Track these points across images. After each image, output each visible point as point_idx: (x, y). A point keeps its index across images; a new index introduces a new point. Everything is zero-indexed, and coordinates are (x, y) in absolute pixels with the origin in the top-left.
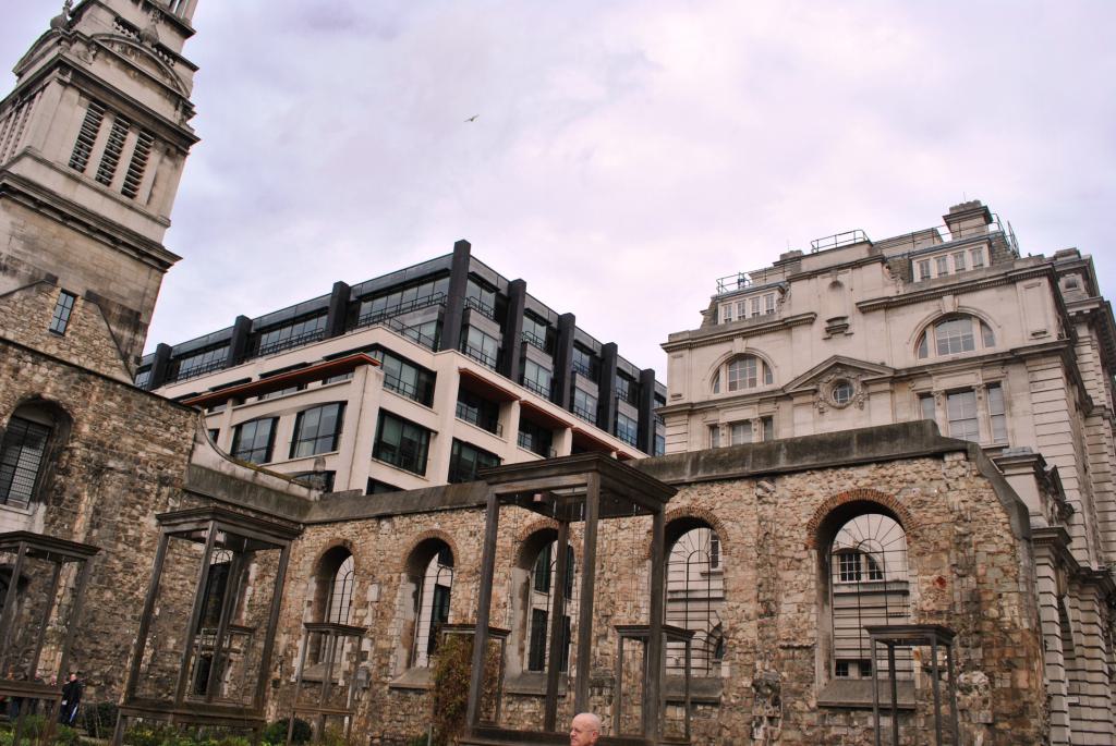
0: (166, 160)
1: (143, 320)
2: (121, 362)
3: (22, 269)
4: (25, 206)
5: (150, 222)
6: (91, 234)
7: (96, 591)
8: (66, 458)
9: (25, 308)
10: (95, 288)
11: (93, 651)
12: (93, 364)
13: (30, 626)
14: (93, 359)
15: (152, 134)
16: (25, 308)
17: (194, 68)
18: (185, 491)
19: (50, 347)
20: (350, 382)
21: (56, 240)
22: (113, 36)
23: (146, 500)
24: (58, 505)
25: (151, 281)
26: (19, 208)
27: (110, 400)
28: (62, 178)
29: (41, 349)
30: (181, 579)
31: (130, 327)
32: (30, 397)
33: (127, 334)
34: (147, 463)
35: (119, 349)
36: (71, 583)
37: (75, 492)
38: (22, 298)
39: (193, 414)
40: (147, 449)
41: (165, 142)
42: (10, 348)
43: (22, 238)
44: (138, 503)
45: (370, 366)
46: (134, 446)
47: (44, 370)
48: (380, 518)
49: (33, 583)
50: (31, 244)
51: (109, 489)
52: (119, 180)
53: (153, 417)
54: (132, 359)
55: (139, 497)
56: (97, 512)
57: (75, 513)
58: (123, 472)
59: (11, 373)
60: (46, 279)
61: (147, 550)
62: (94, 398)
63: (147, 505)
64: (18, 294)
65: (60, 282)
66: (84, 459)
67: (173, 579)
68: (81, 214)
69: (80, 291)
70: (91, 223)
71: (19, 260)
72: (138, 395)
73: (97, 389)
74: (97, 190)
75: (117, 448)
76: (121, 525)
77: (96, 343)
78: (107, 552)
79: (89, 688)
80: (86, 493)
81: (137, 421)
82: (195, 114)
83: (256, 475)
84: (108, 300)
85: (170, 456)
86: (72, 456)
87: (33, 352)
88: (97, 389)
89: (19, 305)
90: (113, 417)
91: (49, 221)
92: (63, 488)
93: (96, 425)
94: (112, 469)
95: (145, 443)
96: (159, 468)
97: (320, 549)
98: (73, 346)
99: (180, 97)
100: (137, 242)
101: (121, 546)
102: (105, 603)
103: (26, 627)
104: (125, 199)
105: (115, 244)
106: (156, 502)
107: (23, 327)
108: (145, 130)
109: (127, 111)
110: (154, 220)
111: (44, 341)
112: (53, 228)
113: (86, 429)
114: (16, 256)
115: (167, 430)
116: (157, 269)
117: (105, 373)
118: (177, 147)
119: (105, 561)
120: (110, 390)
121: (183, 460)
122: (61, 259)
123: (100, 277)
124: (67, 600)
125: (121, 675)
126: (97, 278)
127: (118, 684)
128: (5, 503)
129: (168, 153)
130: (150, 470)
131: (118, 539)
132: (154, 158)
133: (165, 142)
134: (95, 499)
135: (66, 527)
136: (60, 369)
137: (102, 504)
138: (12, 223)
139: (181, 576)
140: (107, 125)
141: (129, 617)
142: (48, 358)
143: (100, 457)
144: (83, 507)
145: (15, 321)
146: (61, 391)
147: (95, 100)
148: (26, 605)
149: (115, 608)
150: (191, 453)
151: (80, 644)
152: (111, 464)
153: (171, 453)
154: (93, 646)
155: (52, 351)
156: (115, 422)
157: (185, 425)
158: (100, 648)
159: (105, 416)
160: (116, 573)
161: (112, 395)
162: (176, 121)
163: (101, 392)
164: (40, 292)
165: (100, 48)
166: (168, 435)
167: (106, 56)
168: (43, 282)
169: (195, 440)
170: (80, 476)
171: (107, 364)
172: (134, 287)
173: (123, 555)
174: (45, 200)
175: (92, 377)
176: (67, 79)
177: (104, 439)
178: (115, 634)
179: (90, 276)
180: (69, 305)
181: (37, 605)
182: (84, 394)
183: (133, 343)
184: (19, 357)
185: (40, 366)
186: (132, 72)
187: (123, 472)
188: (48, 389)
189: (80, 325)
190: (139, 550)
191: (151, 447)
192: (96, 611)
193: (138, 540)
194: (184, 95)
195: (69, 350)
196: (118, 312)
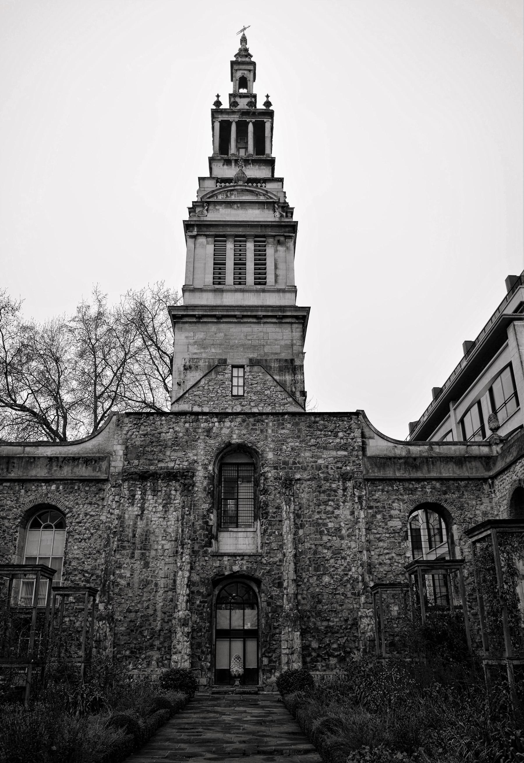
0: (280, 248)
1: (297, 363)
2: (290, 399)
3: (201, 363)
4: (190, 322)
5: (281, 294)
6: (239, 320)
7: (315, 578)
8: (262, 481)
9: (210, 387)
10: (254, 355)
11: (326, 627)
12: (270, 408)
13: (270, 615)
14: (269, 404)
15: (264, 236)
16: (210, 387)
17: (281, 180)
18: (368, 480)
19: (235, 408)
20: (507, 345)
21: (218, 335)
22: (213, 191)
23: (336, 496)
24: (266, 518)
25: (294, 333)
26: (187, 326)
27: (283, 428)
28: (210, 295)
29: (229, 411)
30: (388, 553)
31: (288, 372)
32: (223, 446)
33: (288, 378)
34: (327, 467)
35: (285, 390)
36: (292, 576)
37: (276, 505)
38: (206, 382)
39: (354, 417)
40: (325, 456)
41: (274, 236)
42: (200, 417)
43: (195, 343)
44: (329, 500)
45: (516, 323)
46: (312, 457)
47: (228, 424)
49: (264, 582)
50: (202, 345)
51: (303, 495)
52: (250, 278)
53: (321, 431)
54: (298, 394)
55: (329, 495)
56: (298, 516)
57: (281, 521)
58: (309, 480)
59: (205, 434)
60: (219, 363)
61: (348, 536)
62: (270, 431)
63: (338, 500)
64: (203, 380)
65: (229, 361)
66: (275, 479)
67: (379, 555)
68: (227, 311)
69: (244, 361)
70: (237, 313)
71: (197, 358)
72: (303, 418)
73: (271, 424)
74: (236, 291)
75: (299, 462)
76: (320, 521)
77: (266, 392)
78: (316, 545)
79: (331, 658)
80: (284, 503)
81: (309, 438)
82: (293, 208)
83: (432, 449)
84: (266, 360)
85: (345, 456)
86: (266, 479)
87: (217, 414)
88: (271, 424)
89: (206, 388)
90: (289, 440)
91: (210, 325)
92: (267, 505)
93: (278, 450)
94: (299, 479)
95: (320, 452)
96: (338, 468)
97: (507, 495)
98: (252, 401)
99: (274, 203)
100: (272, 311)
101: (325, 538)
102: (326, 586)
103: (267, 614)
104: (259, 287)
105: (259, 319)
106: (344, 495)
107: (214, 401)
108: (257, 236)
109: (240, 231)
110: (283, 291)
111: (229, 405)
112: (213, 328)
113: (270, 456)
114: (195, 356)
115: (336, 436)
116: (295, 323)
117: (281, 411)
118: (284, 236)
119: (315, 553)
120: (281, 421)
121: (357, 456)
123: (255, 346)
124: (291, 590)
125: (357, 644)
126: (254, 347)
127: (356, 652)
128: (237, 527)
129: (279, 242)
130: (331, 472)
131: (321, 533)
132: (270, 251)
133: (274, 236)
134: (292, 507)
135: (277, 533)
136: (239, 420)
137: (300, 509)
138: (187, 337)
139: (386, 551)
140: (230, 246)
141: (349, 595)
142: (227, 414)
143: (287, 473)
144: (284, 514)
145: (206, 399)
146: (244, 435)
147: (216, 236)
148: (262, 599)
149: (336, 589)
150: (363, 448)
151: (315, 624)
152: (298, 476)
153: (345, 453)
154: (325, 623)
155: (238, 409)
156: (293, 443)
157: (350, 428)
158: (331, 624)
159: (284, 441)
160: (327, 560)
161: (283, 424)
162: (277, 219)
163: (274, 425)
164: (217, 373)
165: (209, 203)
166: (338, 440)
167: (215, 206)
168: (217, 366)
169: (363, 436)
170: (277, 491)
171: (280, 405)
172: (283, 343)
173: (329, 545)
174: (201, 313)
175: (264, 417)
176: (195, 233)
177: (287, 459)
178: (342, 611)
179: (247, 348)
180: (241, 374)
181: (271, 598)
182: (262, 431)
183: (295, 382)
184: (206, 421)
185: (224, 422)
186: (236, 206)
187: (309, 480)
188: (235, 436)
189: (252, 384)
190: (342, 538)
191: (326, 454)
192: (321, 594)
193: (339, 529)
194: (275, 199)
195: (250, 404)
196: (277, 365)
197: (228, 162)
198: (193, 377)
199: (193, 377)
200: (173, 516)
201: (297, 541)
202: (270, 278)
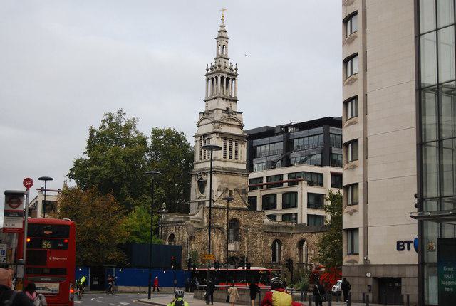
48: (312, 233)
50: (222, 182)
122: (228, 183)
126: (235, 185)
132: (239, 146)
140: (228, 143)
159: (245, 219)
197: (223, 99)
198: (220, 193)
199: (220, 193)
200: (219, 239)
201: (248, 248)
202: (239, 157)
